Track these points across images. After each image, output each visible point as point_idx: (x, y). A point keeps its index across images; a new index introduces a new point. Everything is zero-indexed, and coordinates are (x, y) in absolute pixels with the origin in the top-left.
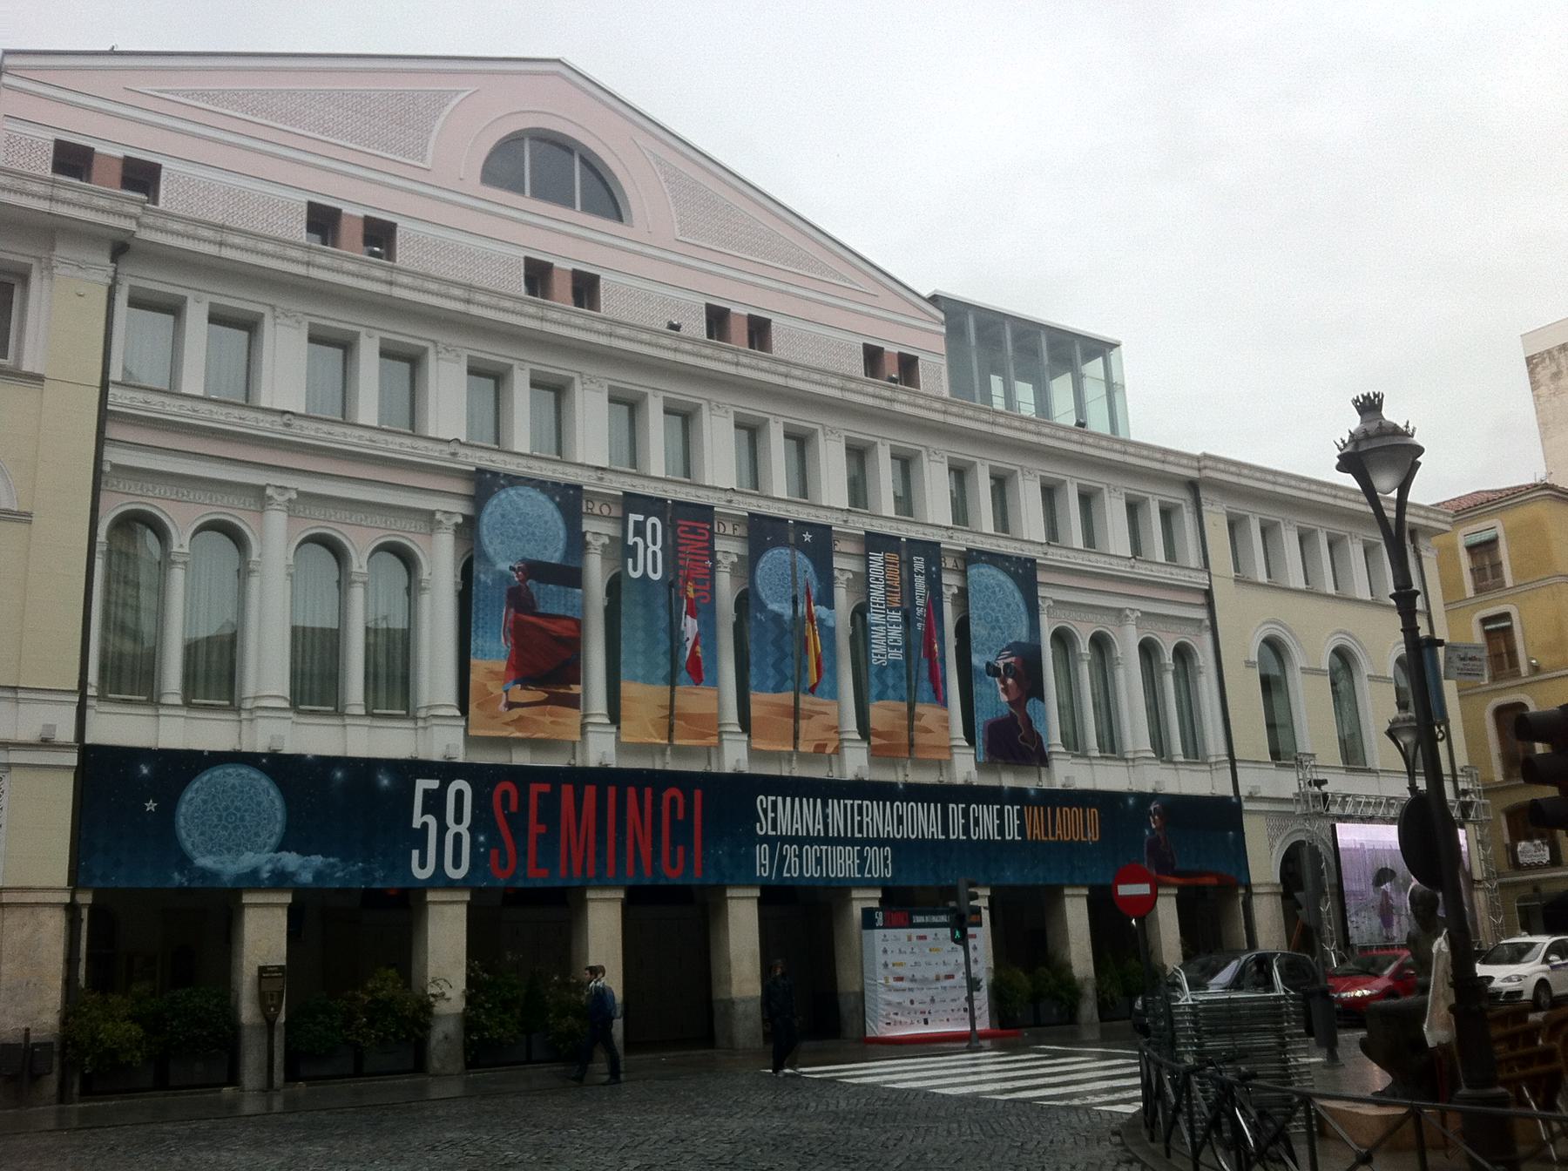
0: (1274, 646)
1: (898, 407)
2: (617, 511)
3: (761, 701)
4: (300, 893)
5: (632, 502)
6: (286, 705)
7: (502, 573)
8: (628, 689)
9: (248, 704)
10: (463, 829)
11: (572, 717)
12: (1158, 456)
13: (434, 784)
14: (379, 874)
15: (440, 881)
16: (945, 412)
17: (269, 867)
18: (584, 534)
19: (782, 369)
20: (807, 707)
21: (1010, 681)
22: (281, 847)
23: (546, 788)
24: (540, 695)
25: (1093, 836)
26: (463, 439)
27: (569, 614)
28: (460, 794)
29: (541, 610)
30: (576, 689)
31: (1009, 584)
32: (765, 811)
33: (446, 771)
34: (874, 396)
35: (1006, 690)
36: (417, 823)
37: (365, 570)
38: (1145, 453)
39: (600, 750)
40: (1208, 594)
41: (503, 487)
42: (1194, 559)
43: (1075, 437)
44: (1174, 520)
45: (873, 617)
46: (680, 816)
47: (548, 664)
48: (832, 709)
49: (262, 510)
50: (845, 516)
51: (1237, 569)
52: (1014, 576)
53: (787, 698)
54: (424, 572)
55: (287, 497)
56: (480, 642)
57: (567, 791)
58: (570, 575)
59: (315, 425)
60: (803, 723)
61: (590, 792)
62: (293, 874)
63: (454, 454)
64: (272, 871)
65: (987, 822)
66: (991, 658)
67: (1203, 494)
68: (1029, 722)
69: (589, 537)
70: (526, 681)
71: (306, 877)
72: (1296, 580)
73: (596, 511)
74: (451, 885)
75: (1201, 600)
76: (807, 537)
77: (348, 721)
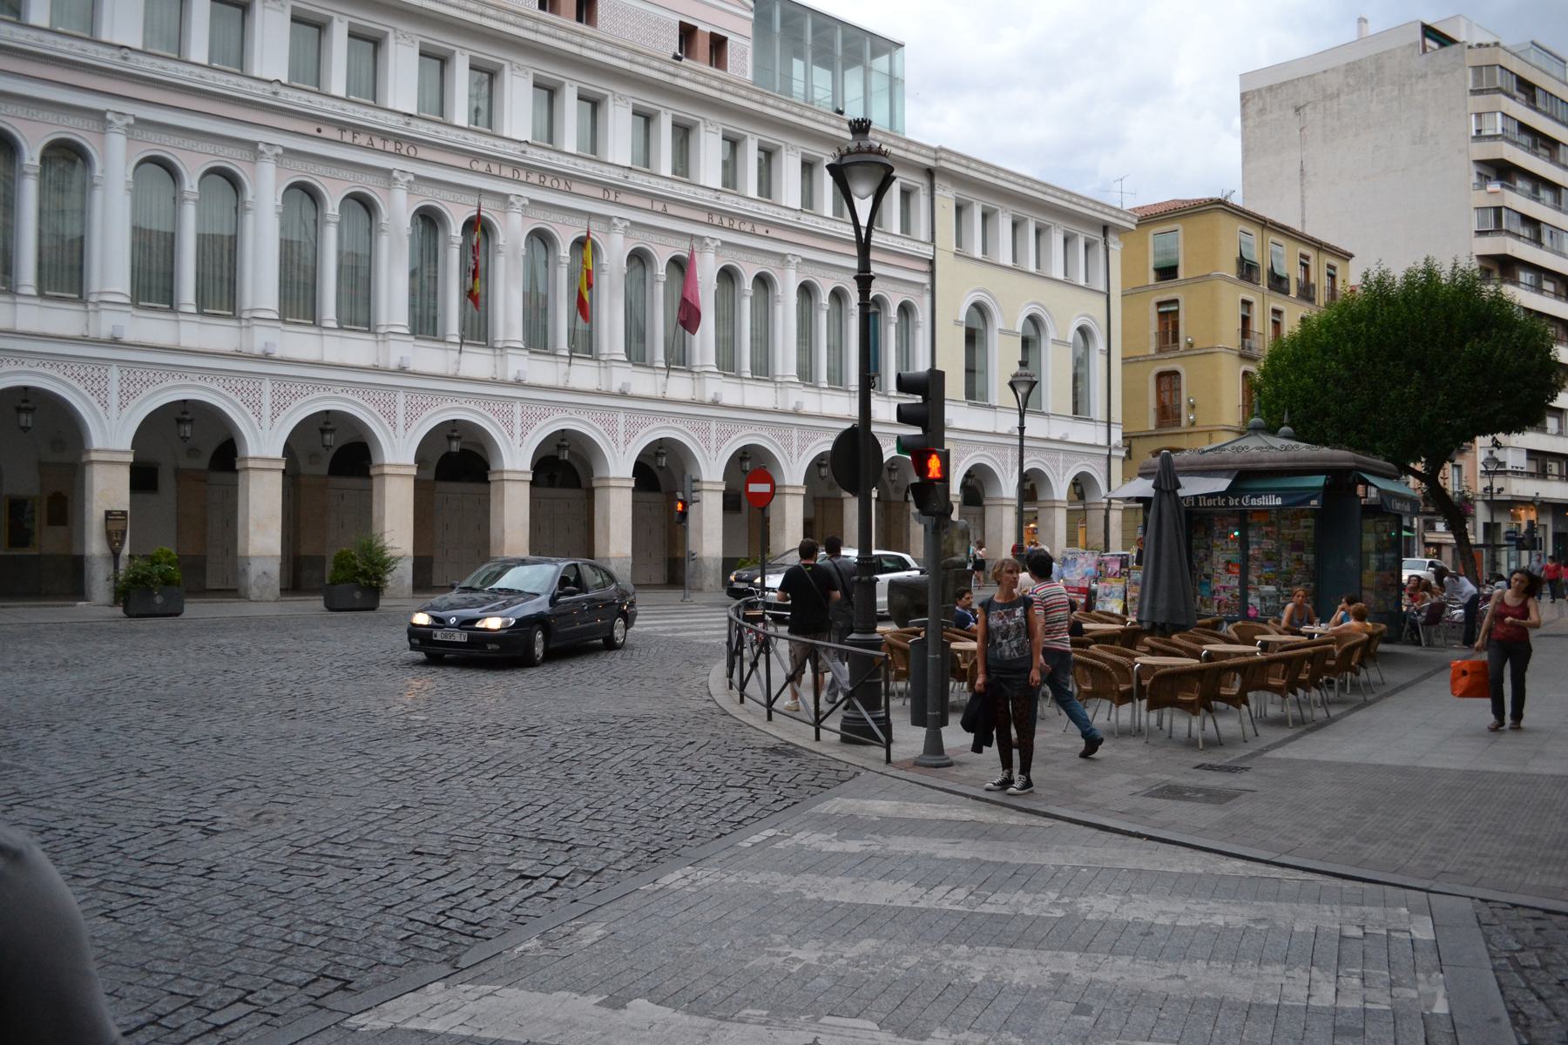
0: (979, 309)
1: (679, 82)
6: (127, 301)
9: (93, 299)
12: (903, 145)
19: (578, 39)
26: (285, 80)
37: (196, 189)
40: (932, 263)
42: (924, 235)
43: (834, 122)
44: (912, 200)
49: (103, 132)
51: (959, 244)
54: (249, 195)
59: (149, 60)
63: (275, 93)
67: (937, 181)
72: (1007, 259)
73: (404, 152)
75: (925, 267)
77: (181, 317)
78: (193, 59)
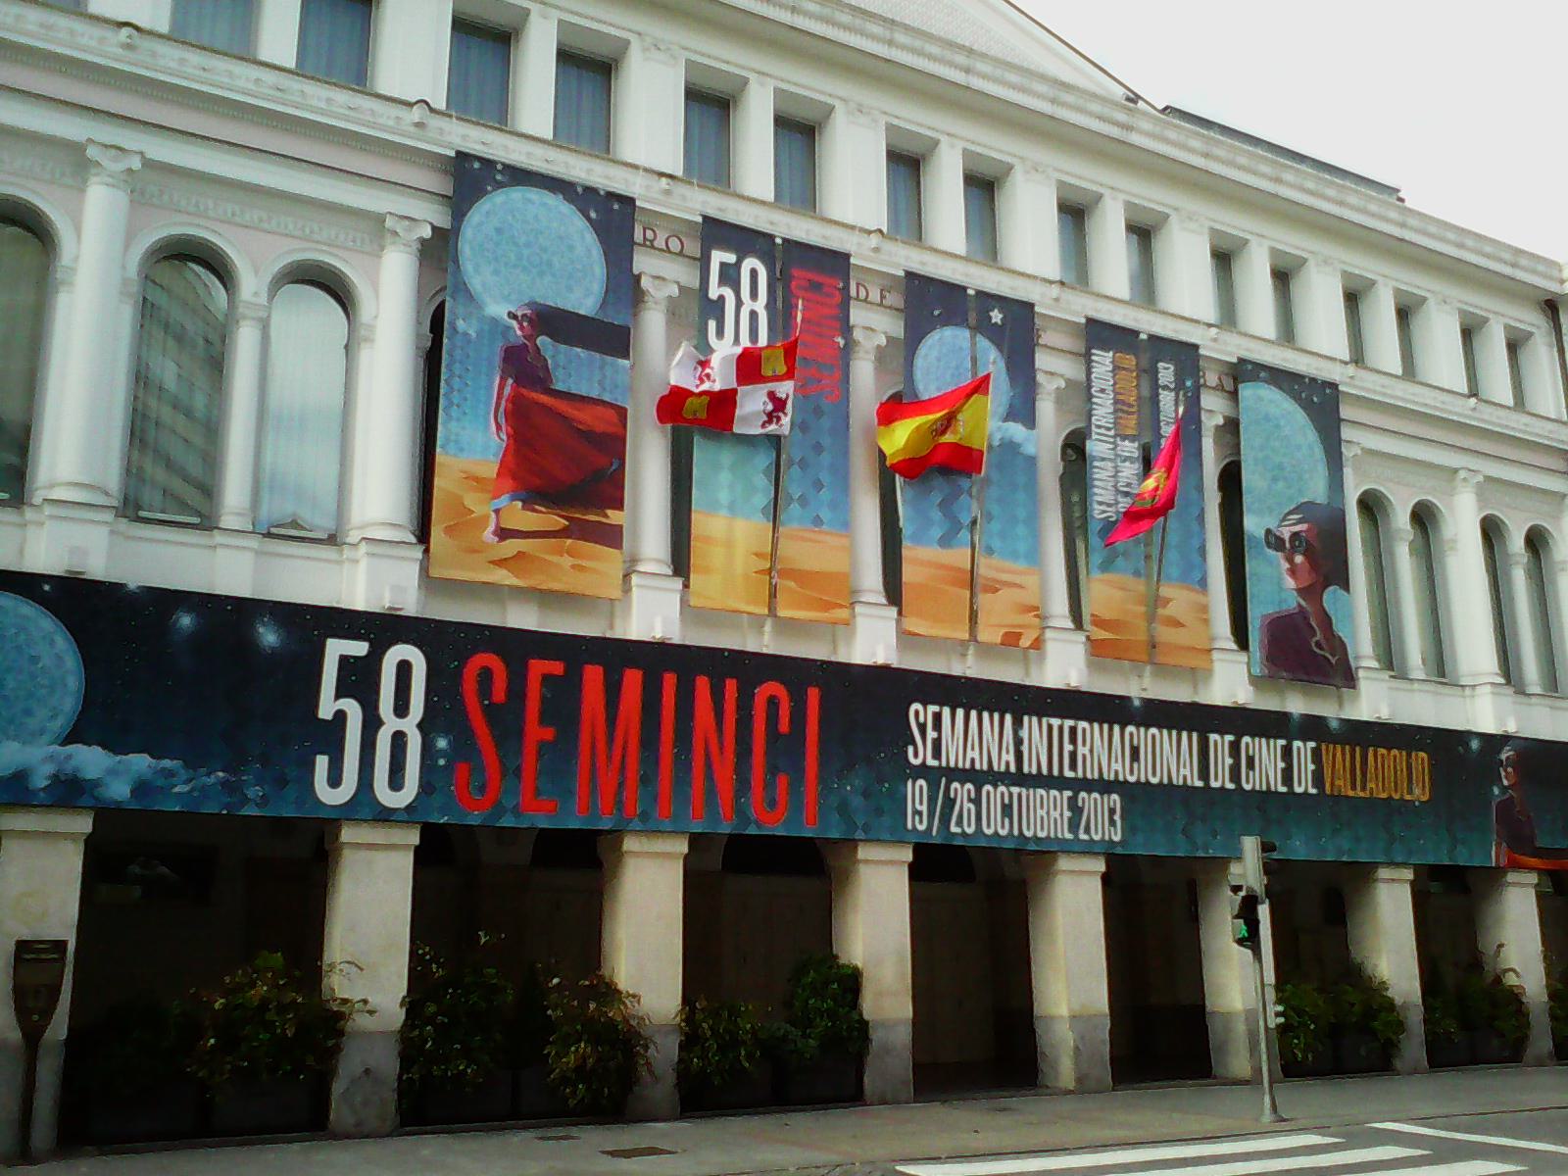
2: (693, 248)
3: (920, 557)
4: (107, 816)
5: (715, 231)
7: (494, 321)
8: (706, 523)
10: (410, 725)
11: (607, 561)
12: (1507, 256)
13: (359, 648)
14: (254, 792)
15: (365, 808)
16: (1206, 155)
17: (49, 769)
18: (638, 278)
19: (960, 59)
20: (992, 574)
21: (1299, 559)
22: (73, 737)
23: (557, 668)
24: (556, 521)
25: (1420, 794)
27: (607, 398)
28: (404, 668)
29: (559, 386)
30: (614, 517)
31: (1300, 416)
32: (922, 728)
33: (382, 628)
34: (1100, 118)
35: (1293, 571)
36: (326, 709)
38: (1488, 249)
39: (652, 614)
41: (500, 185)
45: (1095, 447)
46: (784, 725)
47: (566, 468)
48: (1030, 581)
50: (1055, 290)
52: (1307, 406)
53: (959, 556)
55: (121, 166)
56: (453, 425)
57: (594, 674)
58: (611, 338)
60: (984, 600)
61: (633, 678)
62: (96, 784)
64: (55, 778)
65: (1267, 763)
66: (1272, 526)
68: (1326, 622)
69: (645, 282)
70: (535, 494)
71: (119, 791)
74: (385, 816)
76: (996, 316)
77: (218, 538)
78: (264, 55)
